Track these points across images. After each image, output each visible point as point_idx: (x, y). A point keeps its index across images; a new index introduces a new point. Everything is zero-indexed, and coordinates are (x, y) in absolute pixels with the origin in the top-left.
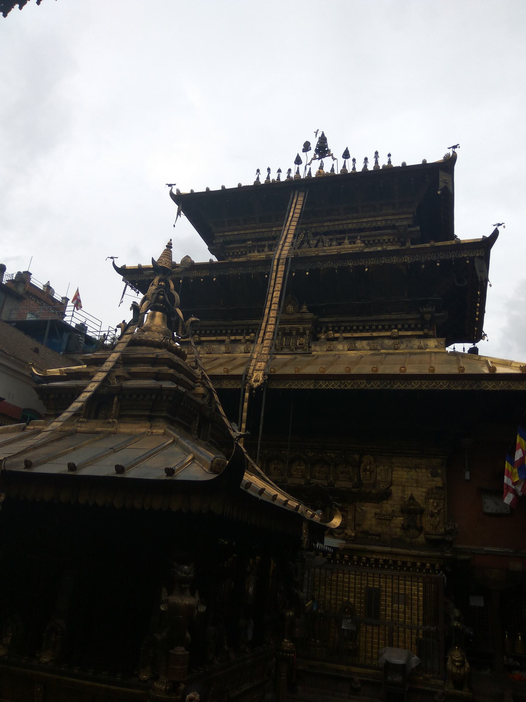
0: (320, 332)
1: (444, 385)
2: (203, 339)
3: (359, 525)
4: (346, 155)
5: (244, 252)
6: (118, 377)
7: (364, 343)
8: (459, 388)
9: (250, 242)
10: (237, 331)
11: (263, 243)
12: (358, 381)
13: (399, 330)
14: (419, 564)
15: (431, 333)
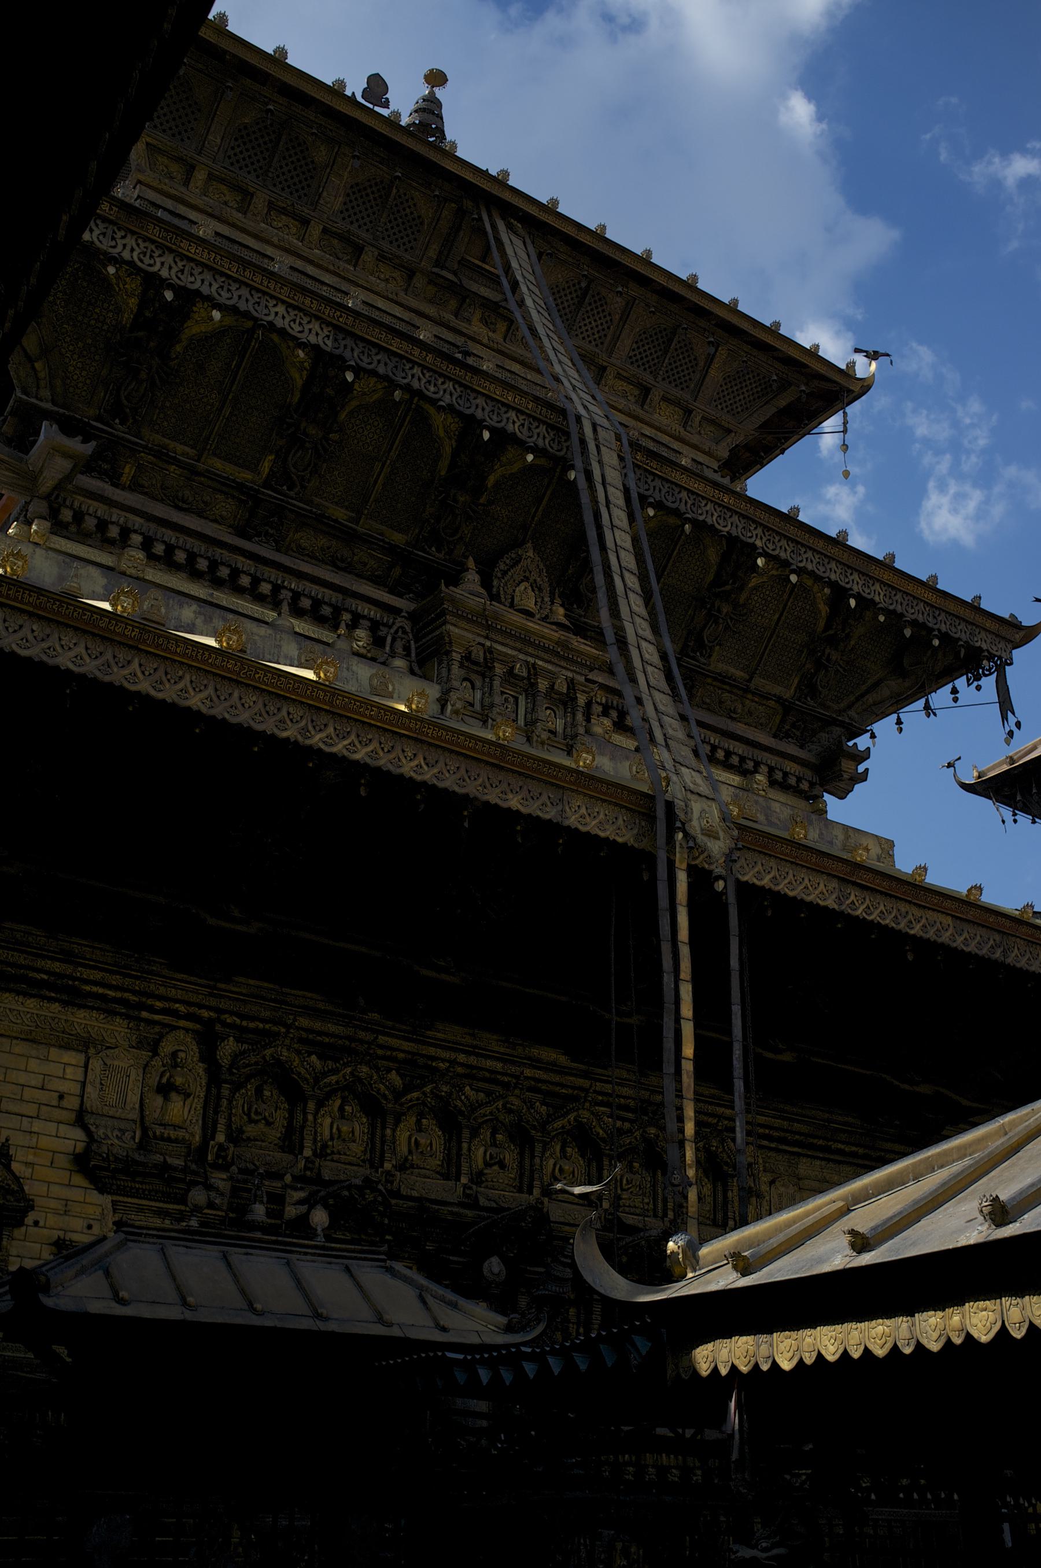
10: (296, 596)
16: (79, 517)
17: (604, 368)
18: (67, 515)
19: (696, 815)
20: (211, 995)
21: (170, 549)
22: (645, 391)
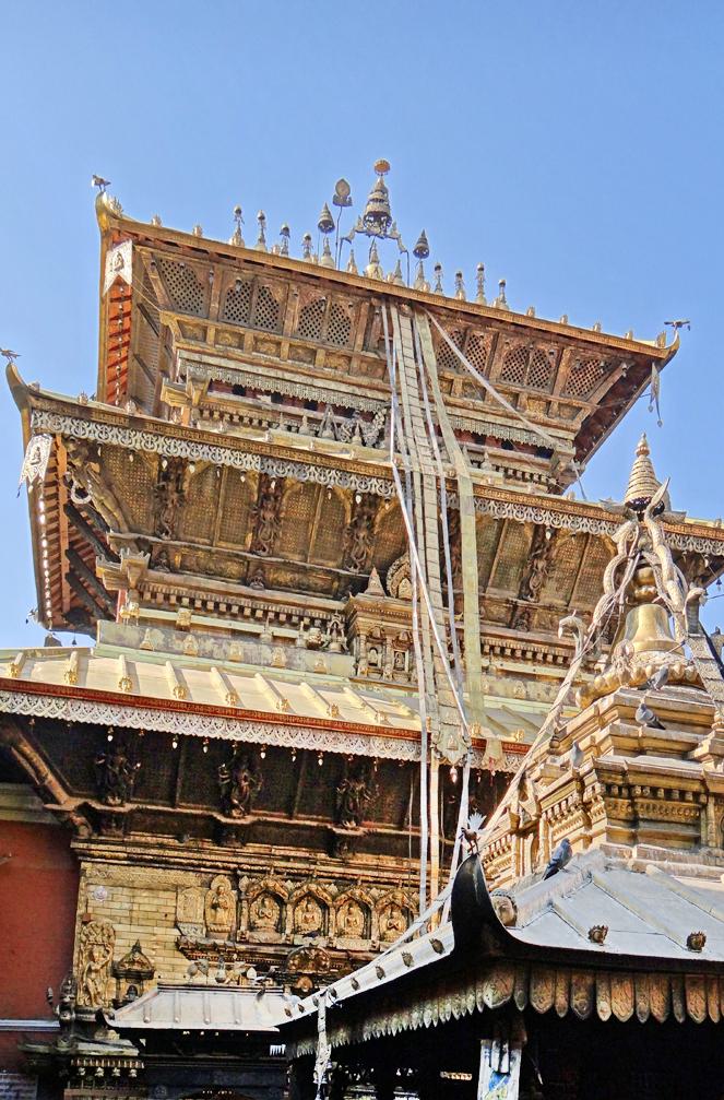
10: (277, 615)
16: (154, 595)
18: (148, 596)
20: (235, 856)
21: (204, 603)
22: (516, 396)
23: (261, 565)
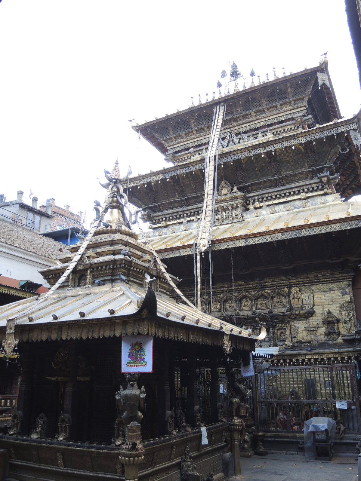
0: (249, 204)
1: (337, 227)
2: (168, 223)
3: (295, 337)
4: (253, 74)
5: (189, 157)
6: (88, 257)
7: (281, 206)
8: (349, 228)
9: (192, 149)
11: (201, 148)
12: (275, 235)
13: (306, 193)
14: (339, 358)
15: (330, 191)
16: (155, 220)
17: (264, 110)
18: (154, 221)
19: (202, 243)
21: (169, 218)
22: (276, 107)
23: (183, 201)
